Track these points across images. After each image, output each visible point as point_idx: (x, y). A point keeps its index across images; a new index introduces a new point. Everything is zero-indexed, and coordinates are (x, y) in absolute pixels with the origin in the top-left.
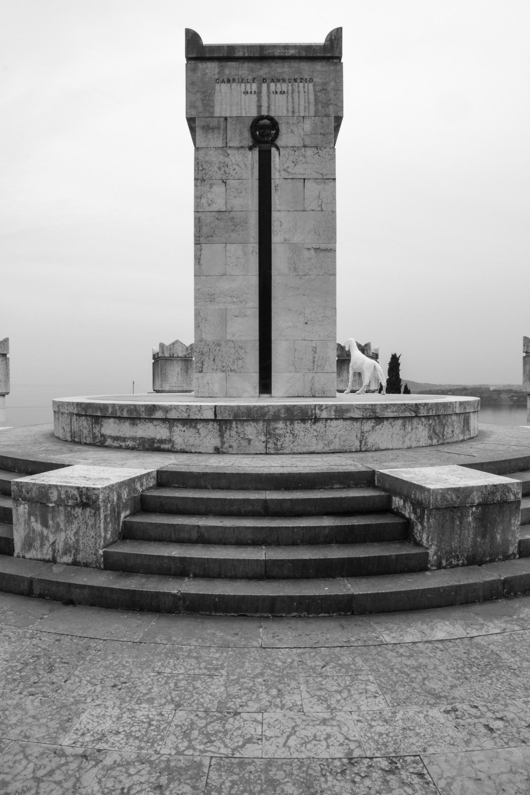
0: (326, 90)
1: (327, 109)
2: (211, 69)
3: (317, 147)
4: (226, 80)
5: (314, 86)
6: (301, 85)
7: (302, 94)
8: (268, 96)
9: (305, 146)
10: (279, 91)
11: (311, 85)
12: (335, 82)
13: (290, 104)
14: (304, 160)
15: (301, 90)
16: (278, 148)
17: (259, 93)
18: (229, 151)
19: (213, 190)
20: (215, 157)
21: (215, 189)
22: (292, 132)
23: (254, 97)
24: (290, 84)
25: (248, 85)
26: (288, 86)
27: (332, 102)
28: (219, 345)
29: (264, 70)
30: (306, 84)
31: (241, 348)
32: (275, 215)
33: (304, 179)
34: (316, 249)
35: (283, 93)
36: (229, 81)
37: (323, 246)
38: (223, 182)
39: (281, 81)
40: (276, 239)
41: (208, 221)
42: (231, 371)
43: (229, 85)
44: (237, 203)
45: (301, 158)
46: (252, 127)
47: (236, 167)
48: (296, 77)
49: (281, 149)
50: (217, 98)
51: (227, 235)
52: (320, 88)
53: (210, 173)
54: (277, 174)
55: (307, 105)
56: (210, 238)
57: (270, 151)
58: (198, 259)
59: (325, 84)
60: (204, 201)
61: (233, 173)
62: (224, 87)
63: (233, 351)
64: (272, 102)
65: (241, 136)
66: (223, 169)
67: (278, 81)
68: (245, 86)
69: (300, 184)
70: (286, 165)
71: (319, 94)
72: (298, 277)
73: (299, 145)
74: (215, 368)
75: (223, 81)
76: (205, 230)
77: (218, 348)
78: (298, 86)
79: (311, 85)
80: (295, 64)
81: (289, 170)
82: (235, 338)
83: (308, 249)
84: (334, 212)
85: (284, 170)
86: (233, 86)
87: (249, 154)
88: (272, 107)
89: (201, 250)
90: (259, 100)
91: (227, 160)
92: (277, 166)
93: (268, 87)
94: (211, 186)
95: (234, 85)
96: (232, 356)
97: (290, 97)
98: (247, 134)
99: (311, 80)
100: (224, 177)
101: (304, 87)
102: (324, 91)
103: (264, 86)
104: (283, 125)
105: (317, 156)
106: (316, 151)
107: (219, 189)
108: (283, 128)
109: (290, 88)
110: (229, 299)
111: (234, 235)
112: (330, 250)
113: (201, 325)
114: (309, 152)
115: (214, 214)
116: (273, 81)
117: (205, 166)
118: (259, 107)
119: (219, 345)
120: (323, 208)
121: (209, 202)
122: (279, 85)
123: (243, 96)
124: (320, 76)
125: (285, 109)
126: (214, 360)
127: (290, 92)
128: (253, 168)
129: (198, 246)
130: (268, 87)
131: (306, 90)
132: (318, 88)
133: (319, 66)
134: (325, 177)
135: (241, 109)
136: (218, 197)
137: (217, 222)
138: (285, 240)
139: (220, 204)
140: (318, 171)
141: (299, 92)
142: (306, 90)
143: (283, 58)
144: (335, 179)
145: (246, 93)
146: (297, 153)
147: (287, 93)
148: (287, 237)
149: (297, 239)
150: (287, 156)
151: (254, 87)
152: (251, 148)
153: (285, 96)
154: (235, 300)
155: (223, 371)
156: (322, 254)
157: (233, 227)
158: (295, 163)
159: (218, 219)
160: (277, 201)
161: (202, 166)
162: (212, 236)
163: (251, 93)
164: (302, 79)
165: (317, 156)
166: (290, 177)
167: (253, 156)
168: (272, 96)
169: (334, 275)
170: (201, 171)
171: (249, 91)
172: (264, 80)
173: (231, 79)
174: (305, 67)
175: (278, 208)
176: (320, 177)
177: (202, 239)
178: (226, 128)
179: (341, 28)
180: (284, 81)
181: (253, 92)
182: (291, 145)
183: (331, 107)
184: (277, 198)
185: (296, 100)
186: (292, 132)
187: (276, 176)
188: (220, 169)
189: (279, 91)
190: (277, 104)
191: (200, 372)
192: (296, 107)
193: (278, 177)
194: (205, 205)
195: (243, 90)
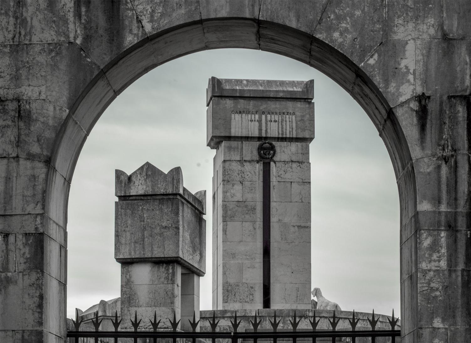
0: (303, 120)
1: (305, 133)
2: (229, 103)
3: (299, 162)
4: (238, 112)
5: (295, 117)
6: (287, 116)
7: (288, 123)
8: (266, 123)
9: (292, 161)
10: (273, 120)
11: (294, 117)
12: (310, 114)
13: (280, 129)
14: (291, 170)
15: (288, 120)
16: (275, 162)
17: (260, 121)
18: (245, 164)
19: (234, 188)
20: (236, 167)
21: (235, 186)
22: (284, 152)
23: (257, 124)
24: (280, 116)
25: (253, 116)
26: (279, 117)
27: (307, 128)
28: (238, 286)
29: (264, 106)
30: (291, 116)
31: (252, 288)
32: (273, 205)
33: (291, 182)
34: (298, 226)
35: (275, 121)
36: (240, 112)
37: (303, 225)
38: (241, 183)
39: (275, 114)
40: (274, 219)
41: (231, 207)
42: (246, 302)
43: (240, 115)
44: (249, 196)
45: (289, 169)
46: (258, 149)
47: (249, 173)
48: (284, 111)
49: (277, 163)
50: (233, 124)
51: (243, 216)
52: (300, 119)
53: (233, 177)
54: (274, 178)
55: (291, 130)
56: (233, 218)
57: (269, 163)
58: (225, 231)
59: (303, 116)
60: (228, 194)
61: (247, 177)
62: (238, 116)
63: (246, 289)
64: (269, 128)
65: (250, 150)
66: (240, 175)
67: (273, 113)
68: (251, 116)
69: (289, 185)
70: (280, 173)
71: (299, 123)
72: (287, 244)
73: (288, 160)
74: (235, 300)
75: (237, 113)
76: (229, 212)
77: (238, 287)
78: (286, 117)
79: (294, 117)
80: (284, 103)
81: (282, 176)
82: (248, 282)
83: (294, 226)
84: (309, 203)
85: (279, 176)
86: (243, 116)
87: (257, 166)
88: (269, 131)
89: (227, 225)
90: (260, 126)
91: (243, 169)
92: (274, 174)
93: (266, 117)
94: (233, 185)
95: (244, 115)
96: (246, 292)
97: (280, 124)
98: (255, 153)
99: (294, 114)
100: (241, 180)
101: (289, 118)
102: (302, 121)
103: (264, 116)
104: (278, 147)
105: (299, 167)
106: (298, 164)
107: (238, 187)
108: (278, 149)
109: (280, 118)
110: (244, 257)
111: (247, 216)
112: (307, 227)
113: (227, 273)
114: (294, 165)
115: (235, 203)
116: (269, 113)
117: (229, 172)
118: (260, 130)
119: (238, 286)
120: (303, 201)
121: (232, 195)
122: (273, 116)
123: (250, 122)
124: (300, 111)
125: (277, 132)
126: (235, 295)
127: (280, 121)
128: (259, 174)
129: (225, 223)
130: (266, 117)
131: (291, 120)
132: (299, 119)
133: (299, 104)
134: (304, 181)
135: (248, 131)
136: (237, 192)
137: (237, 208)
138: (279, 220)
139: (239, 197)
140: (300, 177)
141: (286, 121)
142: (291, 120)
143: (276, 99)
144: (310, 183)
145: (251, 121)
146: (287, 166)
147: (278, 121)
148: (281, 218)
149: (286, 220)
150: (280, 167)
151: (257, 116)
152: (258, 162)
153: (277, 123)
154: (248, 257)
155: (241, 302)
156: (302, 230)
157: (247, 212)
158: (285, 172)
159: (238, 206)
160: (274, 195)
161: (227, 172)
162: (234, 217)
163: (255, 121)
164: (288, 113)
165: (299, 167)
166: (283, 180)
167: (259, 167)
168: (269, 123)
169: (310, 242)
170: (227, 175)
171: (253, 120)
172: (263, 113)
173: (242, 111)
174: (290, 104)
175: (275, 200)
176: (301, 181)
177: (227, 219)
178: (242, 148)
179: (313, 80)
180: (276, 113)
181: (256, 120)
182: (283, 160)
183: (306, 131)
184: (274, 194)
185: (284, 127)
186: (284, 152)
187: (274, 180)
188: (238, 174)
189: (273, 120)
190: (272, 129)
191: (226, 302)
192: (284, 131)
193: (275, 181)
194: (230, 197)
195: (249, 119)
